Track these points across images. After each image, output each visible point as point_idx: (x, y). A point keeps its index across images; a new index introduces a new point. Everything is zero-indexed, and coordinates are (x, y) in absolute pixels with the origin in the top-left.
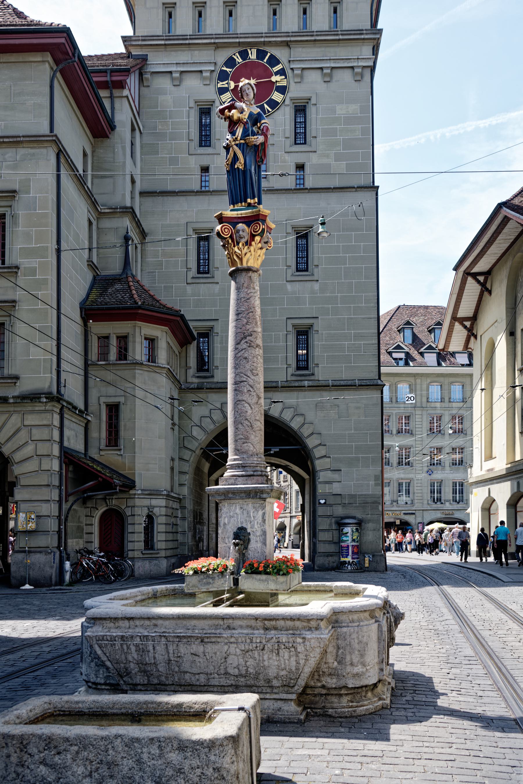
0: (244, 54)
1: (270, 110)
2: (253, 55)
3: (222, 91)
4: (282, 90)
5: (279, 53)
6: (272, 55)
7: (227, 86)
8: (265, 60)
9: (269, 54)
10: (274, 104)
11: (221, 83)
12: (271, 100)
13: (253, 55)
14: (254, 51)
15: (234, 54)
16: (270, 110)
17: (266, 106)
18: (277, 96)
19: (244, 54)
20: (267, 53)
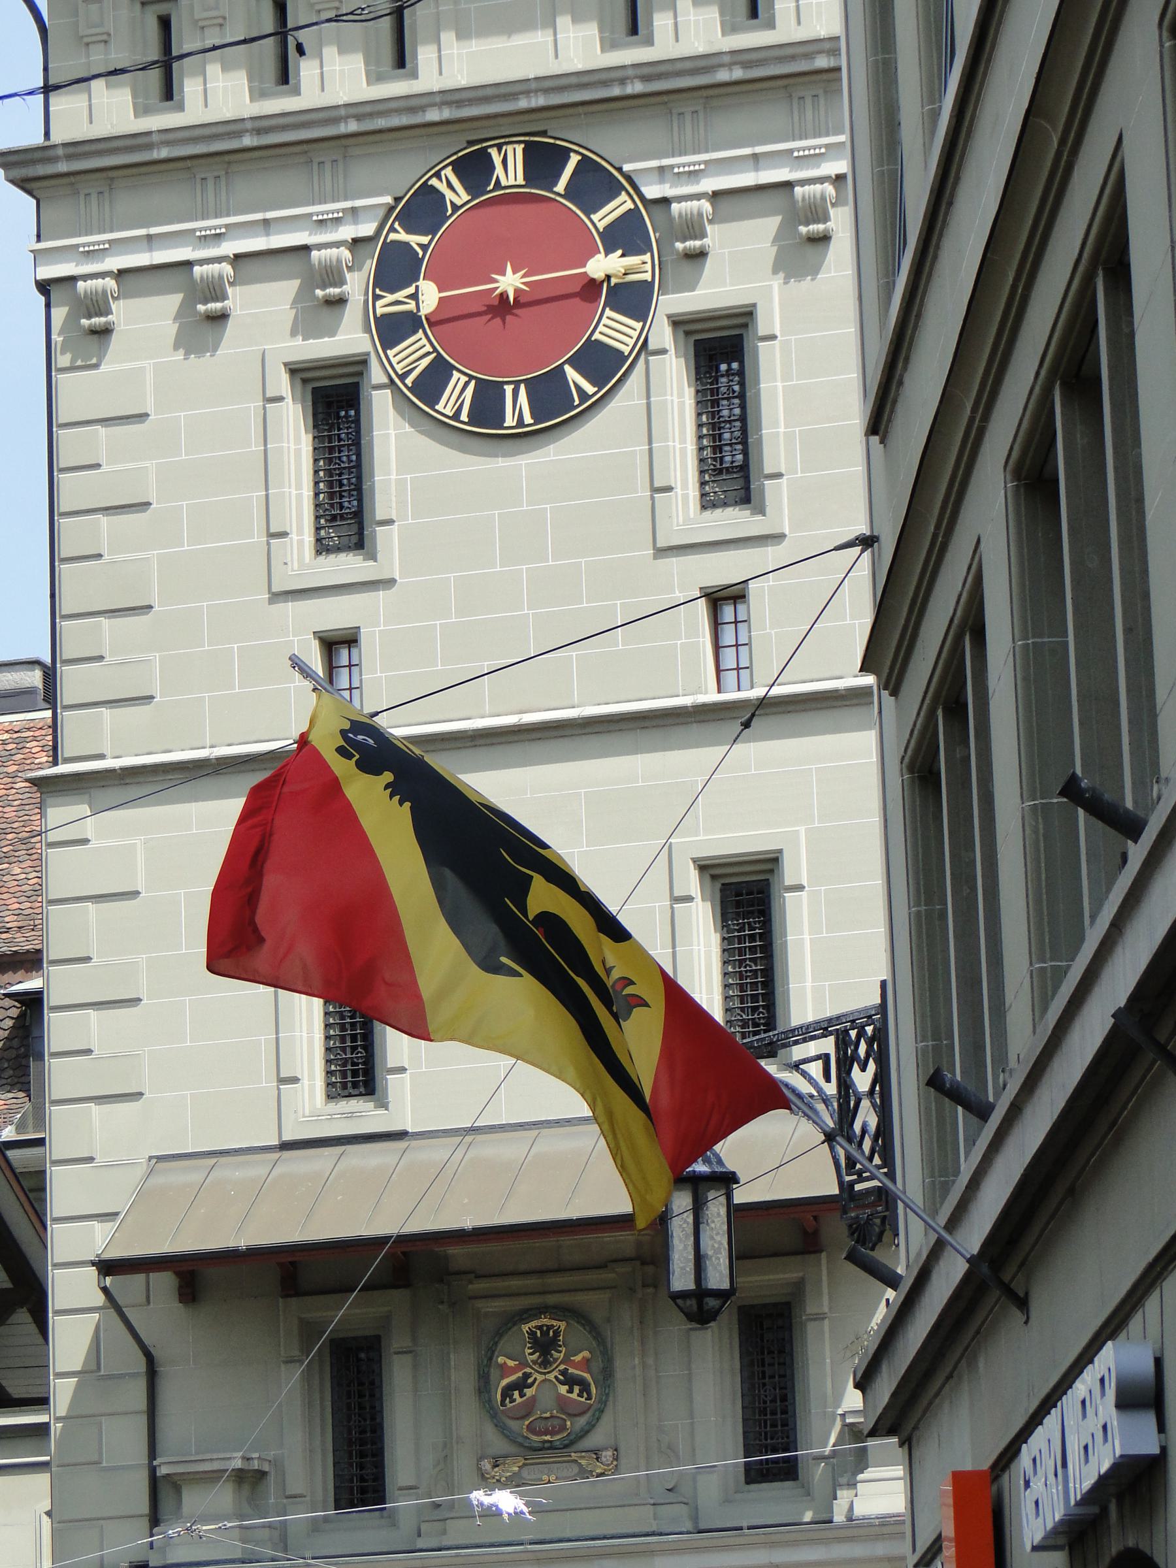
0: (473, 170)
1: (590, 389)
2: (510, 169)
3: (393, 329)
4: (632, 299)
5: (610, 144)
6: (585, 162)
7: (412, 306)
8: (561, 187)
9: (574, 159)
11: (390, 298)
13: (510, 169)
14: (516, 154)
15: (437, 175)
16: (590, 389)
17: (571, 373)
18: (614, 329)
19: (473, 170)
20: (565, 154)
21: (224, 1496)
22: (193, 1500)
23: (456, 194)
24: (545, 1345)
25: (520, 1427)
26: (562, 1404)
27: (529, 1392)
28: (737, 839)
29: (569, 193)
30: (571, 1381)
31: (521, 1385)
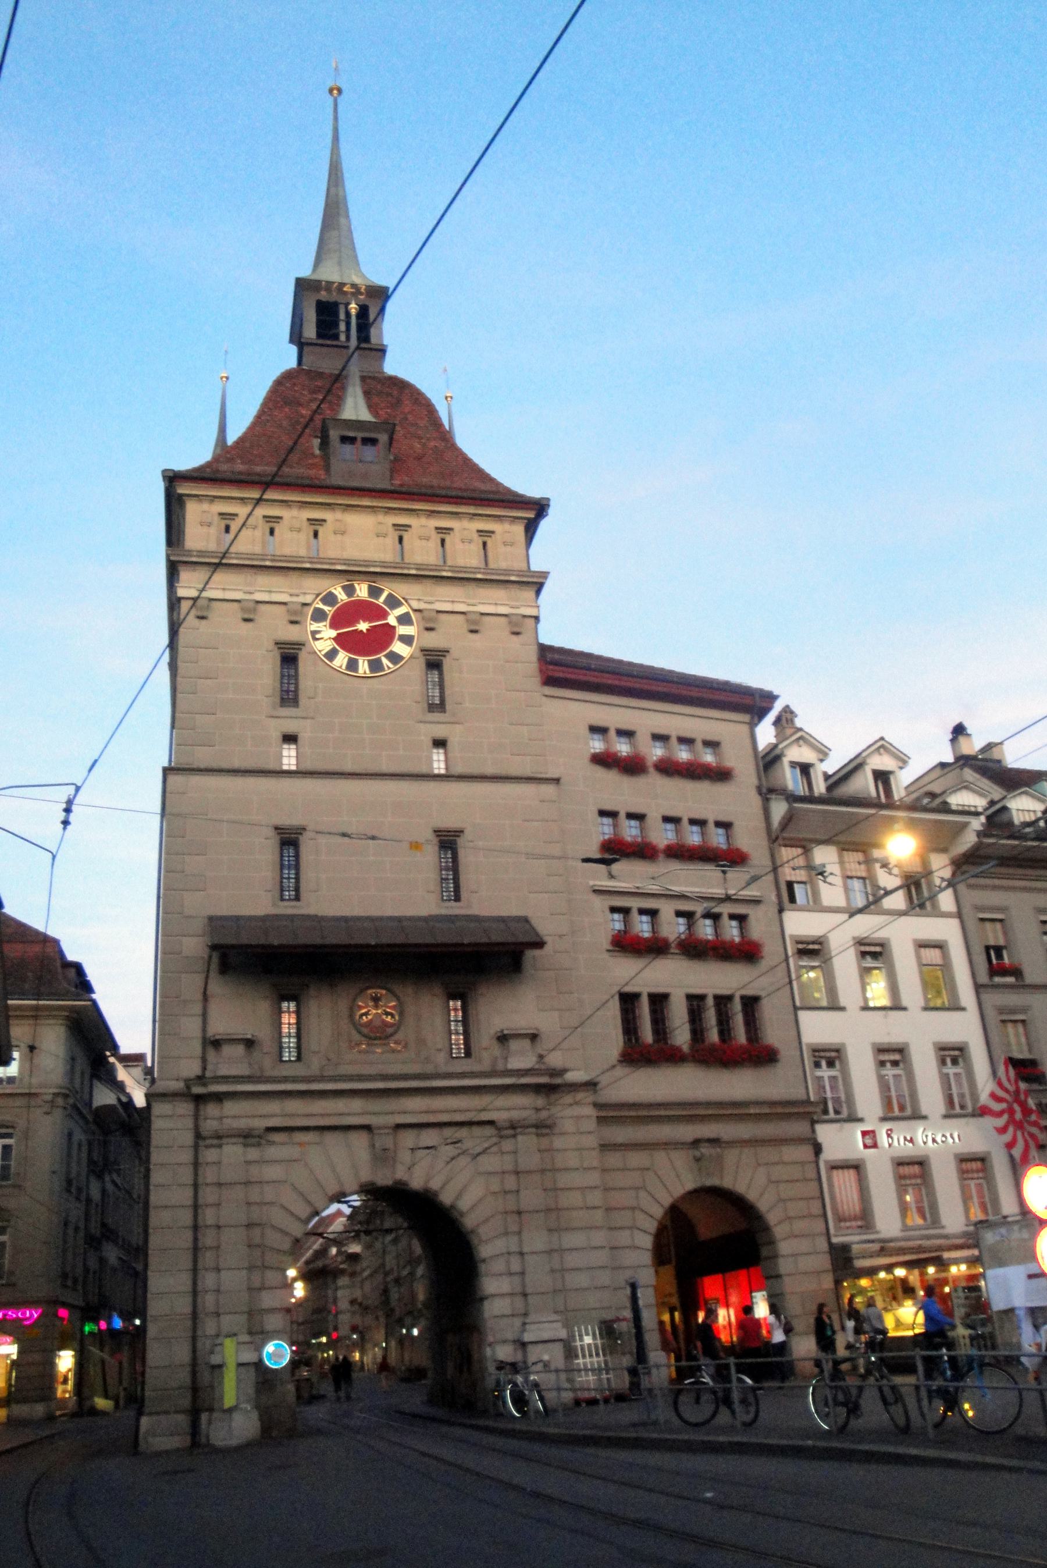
4: (407, 640)
6: (390, 596)
10: (395, 658)
12: (392, 652)
13: (362, 591)
16: (391, 665)
19: (349, 590)
20: (381, 591)
21: (240, 1049)
22: (227, 1050)
23: (342, 596)
24: (376, 1000)
25: (365, 1031)
26: (383, 1021)
27: (370, 1017)
28: (449, 822)
29: (385, 602)
30: (387, 1014)
31: (366, 1014)
